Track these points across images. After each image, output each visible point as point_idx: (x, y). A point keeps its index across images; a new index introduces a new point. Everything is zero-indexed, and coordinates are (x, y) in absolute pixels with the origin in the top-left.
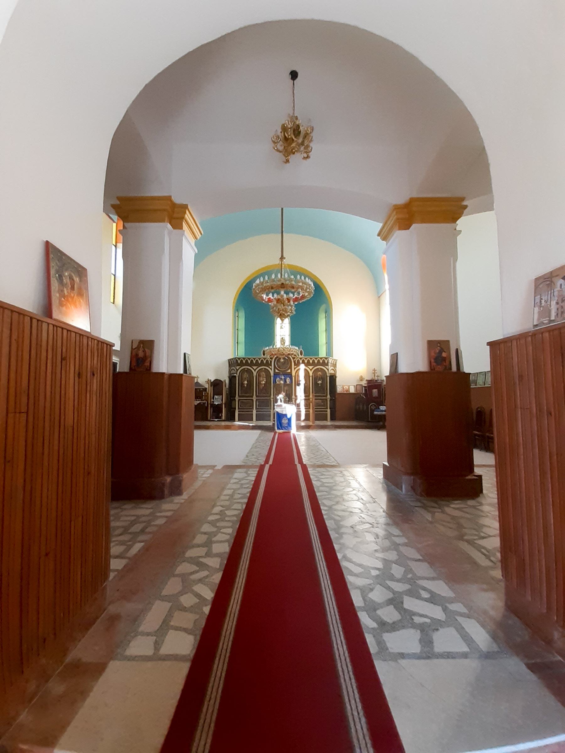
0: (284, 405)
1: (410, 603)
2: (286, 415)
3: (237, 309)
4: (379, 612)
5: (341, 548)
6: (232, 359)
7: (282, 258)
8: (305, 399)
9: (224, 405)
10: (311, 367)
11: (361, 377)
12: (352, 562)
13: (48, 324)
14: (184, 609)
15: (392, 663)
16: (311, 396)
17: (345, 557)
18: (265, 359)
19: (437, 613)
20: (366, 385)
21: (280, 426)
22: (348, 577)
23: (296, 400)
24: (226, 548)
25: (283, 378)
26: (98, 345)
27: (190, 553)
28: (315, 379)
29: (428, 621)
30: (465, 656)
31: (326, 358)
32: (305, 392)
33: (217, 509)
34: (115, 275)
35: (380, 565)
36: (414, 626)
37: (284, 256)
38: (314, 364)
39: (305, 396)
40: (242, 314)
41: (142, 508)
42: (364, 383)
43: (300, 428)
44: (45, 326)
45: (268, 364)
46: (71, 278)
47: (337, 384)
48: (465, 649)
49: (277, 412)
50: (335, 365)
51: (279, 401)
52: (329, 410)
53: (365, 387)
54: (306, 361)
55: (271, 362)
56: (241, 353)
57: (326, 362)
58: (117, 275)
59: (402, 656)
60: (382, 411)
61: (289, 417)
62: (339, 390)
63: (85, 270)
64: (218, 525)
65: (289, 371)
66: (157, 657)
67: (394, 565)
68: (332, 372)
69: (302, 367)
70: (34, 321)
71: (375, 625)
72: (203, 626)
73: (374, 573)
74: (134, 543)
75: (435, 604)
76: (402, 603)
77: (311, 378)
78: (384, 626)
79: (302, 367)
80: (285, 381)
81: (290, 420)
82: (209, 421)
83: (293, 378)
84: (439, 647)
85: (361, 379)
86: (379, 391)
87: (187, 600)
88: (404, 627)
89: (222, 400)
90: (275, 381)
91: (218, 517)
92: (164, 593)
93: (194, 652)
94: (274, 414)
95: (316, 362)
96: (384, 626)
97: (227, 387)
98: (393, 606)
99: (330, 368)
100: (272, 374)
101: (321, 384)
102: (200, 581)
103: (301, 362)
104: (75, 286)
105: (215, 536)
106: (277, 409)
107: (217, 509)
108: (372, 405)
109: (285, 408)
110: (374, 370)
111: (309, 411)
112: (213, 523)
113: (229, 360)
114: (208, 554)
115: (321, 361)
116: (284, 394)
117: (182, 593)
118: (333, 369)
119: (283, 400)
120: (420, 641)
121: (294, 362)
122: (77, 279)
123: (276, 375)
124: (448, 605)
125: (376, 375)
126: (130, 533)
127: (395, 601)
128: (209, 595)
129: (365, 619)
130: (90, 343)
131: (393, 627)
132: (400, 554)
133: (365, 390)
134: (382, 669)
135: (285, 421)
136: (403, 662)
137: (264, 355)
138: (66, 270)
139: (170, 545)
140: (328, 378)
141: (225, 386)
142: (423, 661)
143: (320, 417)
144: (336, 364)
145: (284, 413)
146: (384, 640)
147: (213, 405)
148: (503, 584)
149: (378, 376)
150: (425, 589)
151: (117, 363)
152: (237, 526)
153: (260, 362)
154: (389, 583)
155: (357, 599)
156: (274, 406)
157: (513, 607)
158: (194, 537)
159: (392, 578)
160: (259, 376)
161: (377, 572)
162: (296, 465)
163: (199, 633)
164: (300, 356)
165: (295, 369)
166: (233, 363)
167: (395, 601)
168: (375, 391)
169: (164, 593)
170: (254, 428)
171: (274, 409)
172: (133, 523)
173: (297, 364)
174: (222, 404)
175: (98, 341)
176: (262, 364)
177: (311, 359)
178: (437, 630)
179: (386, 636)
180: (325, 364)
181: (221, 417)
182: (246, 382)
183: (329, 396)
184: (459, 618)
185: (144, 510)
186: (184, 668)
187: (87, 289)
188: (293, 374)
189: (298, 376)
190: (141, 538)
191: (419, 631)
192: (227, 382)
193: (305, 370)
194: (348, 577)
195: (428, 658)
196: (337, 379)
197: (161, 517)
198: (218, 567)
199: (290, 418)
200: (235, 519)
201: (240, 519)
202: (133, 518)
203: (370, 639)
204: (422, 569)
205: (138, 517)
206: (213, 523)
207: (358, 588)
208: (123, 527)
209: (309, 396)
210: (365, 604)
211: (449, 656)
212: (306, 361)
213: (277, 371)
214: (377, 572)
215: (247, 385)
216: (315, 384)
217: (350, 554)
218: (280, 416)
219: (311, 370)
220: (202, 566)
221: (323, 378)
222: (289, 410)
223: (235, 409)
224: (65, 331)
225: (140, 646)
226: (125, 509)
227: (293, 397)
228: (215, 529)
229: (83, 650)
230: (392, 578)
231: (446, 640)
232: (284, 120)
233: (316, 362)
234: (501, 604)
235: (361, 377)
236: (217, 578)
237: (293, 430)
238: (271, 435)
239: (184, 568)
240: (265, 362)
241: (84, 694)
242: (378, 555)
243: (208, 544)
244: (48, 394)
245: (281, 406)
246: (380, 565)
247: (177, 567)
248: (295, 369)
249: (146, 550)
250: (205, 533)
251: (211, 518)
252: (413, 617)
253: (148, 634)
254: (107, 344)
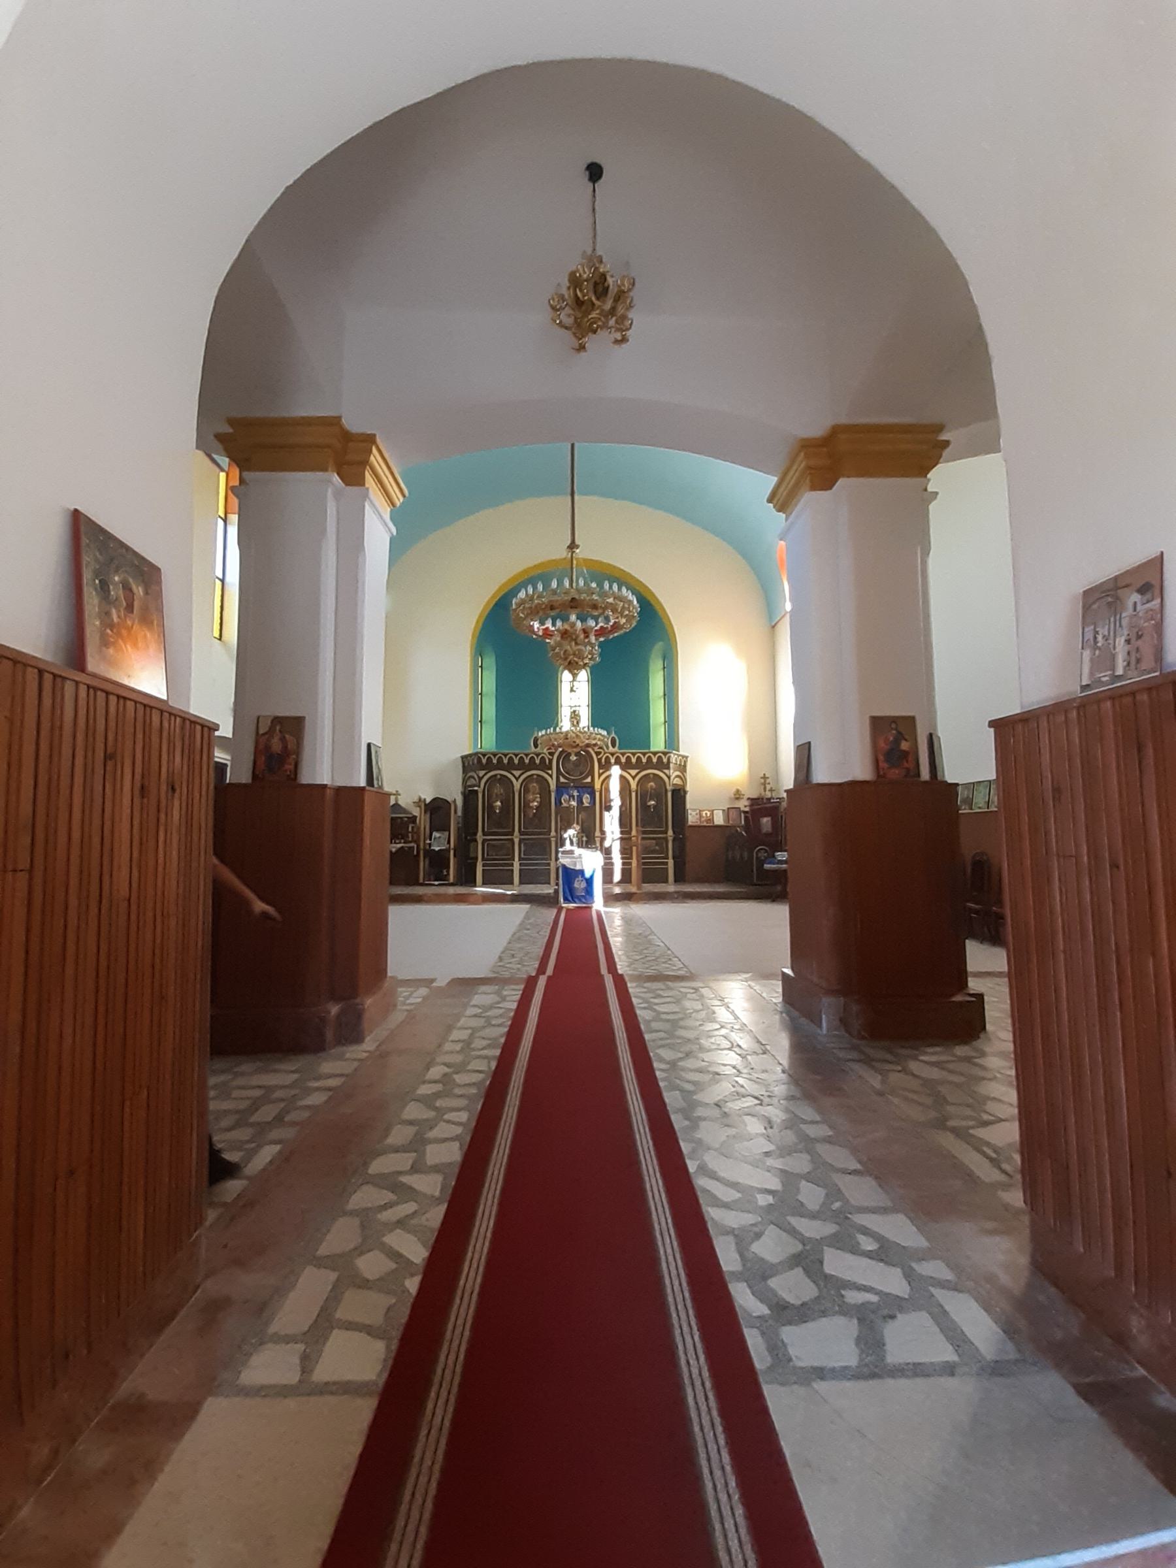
0: (578, 851)
1: (837, 1263)
2: (582, 872)
3: (479, 651)
4: (773, 1283)
5: (694, 1151)
6: (470, 755)
7: (573, 546)
8: (622, 839)
9: (452, 852)
10: (633, 772)
11: (738, 791)
12: (718, 1179)
13: (77, 683)
14: (365, 1284)
15: (800, 1390)
16: (634, 833)
17: (703, 1169)
18: (538, 755)
19: (893, 1282)
20: (747, 809)
21: (571, 895)
22: (709, 1209)
23: (603, 840)
24: (452, 1154)
25: (576, 794)
26: (182, 728)
27: (378, 1166)
28: (643, 796)
29: (874, 1298)
30: (949, 1370)
31: (665, 754)
32: (622, 824)
33: (436, 1072)
34: (223, 581)
35: (775, 1184)
36: (845, 1310)
37: (577, 542)
38: (639, 765)
39: (622, 833)
40: (490, 662)
41: (275, 1071)
42: (743, 805)
43: (610, 899)
44: (69, 688)
45: (545, 766)
46: (127, 588)
47: (688, 806)
48: (948, 1355)
49: (564, 867)
50: (683, 768)
51: (568, 842)
52: (671, 862)
53: (745, 812)
54: (623, 760)
55: (551, 761)
56: (488, 742)
57: (665, 760)
58: (227, 580)
59: (821, 1373)
60: (781, 862)
61: (587, 875)
62: (692, 819)
63: (159, 570)
64: (438, 1104)
65: (589, 780)
66: (306, 1388)
67: (804, 1182)
68: (677, 781)
69: (616, 771)
70: (48, 678)
71: (762, 1309)
72: (404, 1320)
73: (763, 1200)
74: (260, 1146)
75: (886, 1263)
76: (821, 1263)
77: (634, 794)
78: (784, 1312)
79: (616, 771)
80: (580, 802)
81: (590, 882)
82: (422, 885)
83: (597, 794)
84: (895, 1354)
85: (738, 795)
86: (775, 824)
87: (372, 1265)
88: (824, 1313)
89: (449, 842)
90: (558, 802)
91: (438, 1087)
92: (323, 1251)
93: (385, 1375)
94: (557, 869)
95: (644, 760)
96: (784, 1312)
97: (460, 813)
98: (800, 1269)
99: (673, 773)
100: (553, 786)
101: (655, 807)
102: (401, 1223)
103: (613, 761)
104: (136, 603)
105: (431, 1128)
106: (564, 861)
107: (436, 1072)
108: (760, 851)
109: (580, 857)
110: (764, 777)
111: (630, 864)
112: (428, 1101)
113: (462, 757)
114: (415, 1169)
115: (655, 760)
116: (578, 828)
117: (360, 1251)
118: (677, 776)
119: (575, 840)
120: (858, 1341)
121: (599, 761)
122: (139, 591)
123: (561, 788)
124: (914, 1265)
125: (768, 787)
126: (252, 1125)
127: (807, 1260)
128: (418, 1253)
129: (744, 1298)
130: (166, 724)
131: (801, 1314)
132: (816, 1159)
133: (746, 818)
134: (781, 1402)
135: (579, 885)
136: (820, 1386)
137: (536, 746)
138: (116, 571)
139: (339, 1147)
140: (669, 794)
141: (456, 812)
142: (862, 1384)
143: (652, 874)
144: (685, 766)
145: (578, 867)
146: (782, 1341)
147: (429, 853)
148: (1026, 1220)
149: (771, 790)
150: (866, 1231)
151: (226, 765)
152: (479, 1107)
153: (527, 761)
154: (794, 1221)
155: (728, 1258)
156: (557, 852)
157: (1047, 1265)
158: (387, 1132)
159: (800, 1210)
160: (527, 791)
161: (770, 1199)
162: (602, 977)
163: (396, 1334)
164: (611, 749)
165: (600, 775)
166: (472, 764)
167: (807, 1260)
168: (766, 821)
169: (323, 1251)
170: (515, 899)
171: (557, 859)
172: (255, 1105)
173: (606, 766)
174: (448, 850)
175: (184, 719)
176: (532, 765)
177: (634, 754)
178: (893, 1317)
179: (788, 1333)
180: (663, 765)
181: (446, 878)
182: (499, 803)
183: (670, 832)
184: (938, 1293)
185: (281, 1076)
186: (364, 1410)
187: (160, 610)
188: (597, 786)
189: (608, 790)
190: (275, 1134)
191: (855, 1321)
192: (460, 803)
193: (622, 777)
194: (709, 1209)
195: (874, 1376)
196: (688, 797)
197: (318, 1089)
198: (437, 1194)
199: (592, 877)
200: (474, 1091)
201: (483, 1091)
202: (257, 1093)
203: (753, 1340)
204: (861, 1191)
205: (269, 1089)
206: (428, 1101)
207: (730, 1232)
208: (237, 1112)
209: (630, 832)
210: (744, 1265)
211: (918, 1370)
212: (623, 760)
213: (562, 780)
214: (770, 1199)
215: (501, 809)
216: (643, 806)
217: (712, 1161)
218: (570, 875)
219: (634, 778)
220: (405, 1192)
221: (659, 794)
222: (590, 862)
223: (477, 858)
224: (113, 699)
225: (270, 1365)
226: (243, 1074)
227: (598, 833)
228: (432, 1114)
229: (149, 1376)
230: (800, 1210)
231: (911, 1339)
232: (574, 263)
233: (644, 760)
234: (1024, 1260)
235: (738, 791)
236: (436, 1216)
237: (598, 903)
238: (550, 914)
239: (364, 1197)
240: (538, 761)
241: (151, 1468)
242: (770, 1162)
243: (418, 1144)
244: (76, 835)
245: (572, 852)
246: (775, 1184)
247: (351, 1195)
248: (600, 775)
249: (285, 1159)
250: (411, 1123)
251: (425, 1090)
252: (843, 1292)
253: (288, 1339)
254: (203, 726)
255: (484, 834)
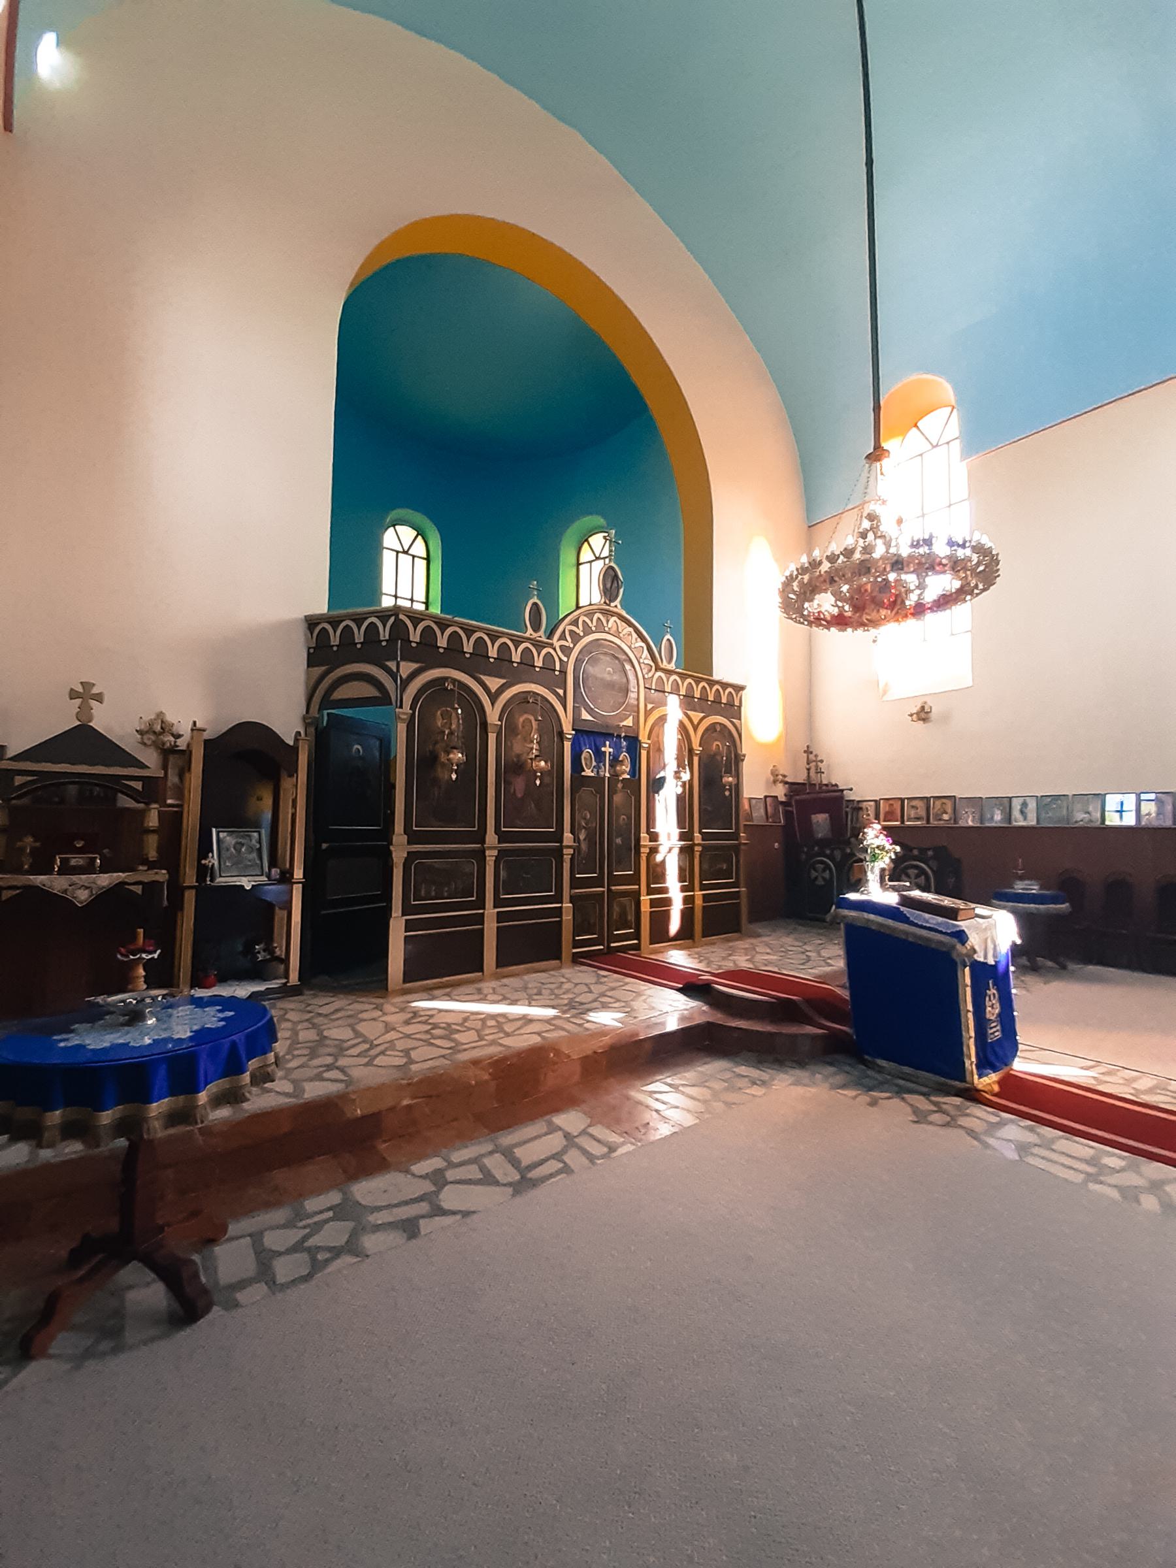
53: (782, 803)
83: (644, 753)
133: (788, 815)
213: (585, 716)
255: (413, 837)
